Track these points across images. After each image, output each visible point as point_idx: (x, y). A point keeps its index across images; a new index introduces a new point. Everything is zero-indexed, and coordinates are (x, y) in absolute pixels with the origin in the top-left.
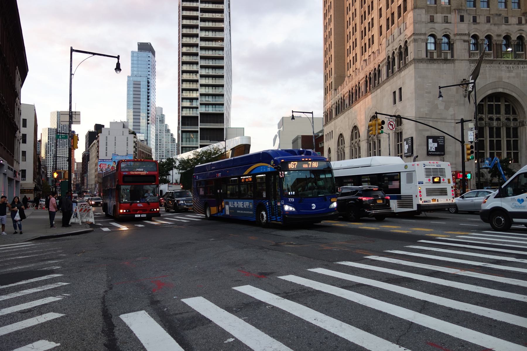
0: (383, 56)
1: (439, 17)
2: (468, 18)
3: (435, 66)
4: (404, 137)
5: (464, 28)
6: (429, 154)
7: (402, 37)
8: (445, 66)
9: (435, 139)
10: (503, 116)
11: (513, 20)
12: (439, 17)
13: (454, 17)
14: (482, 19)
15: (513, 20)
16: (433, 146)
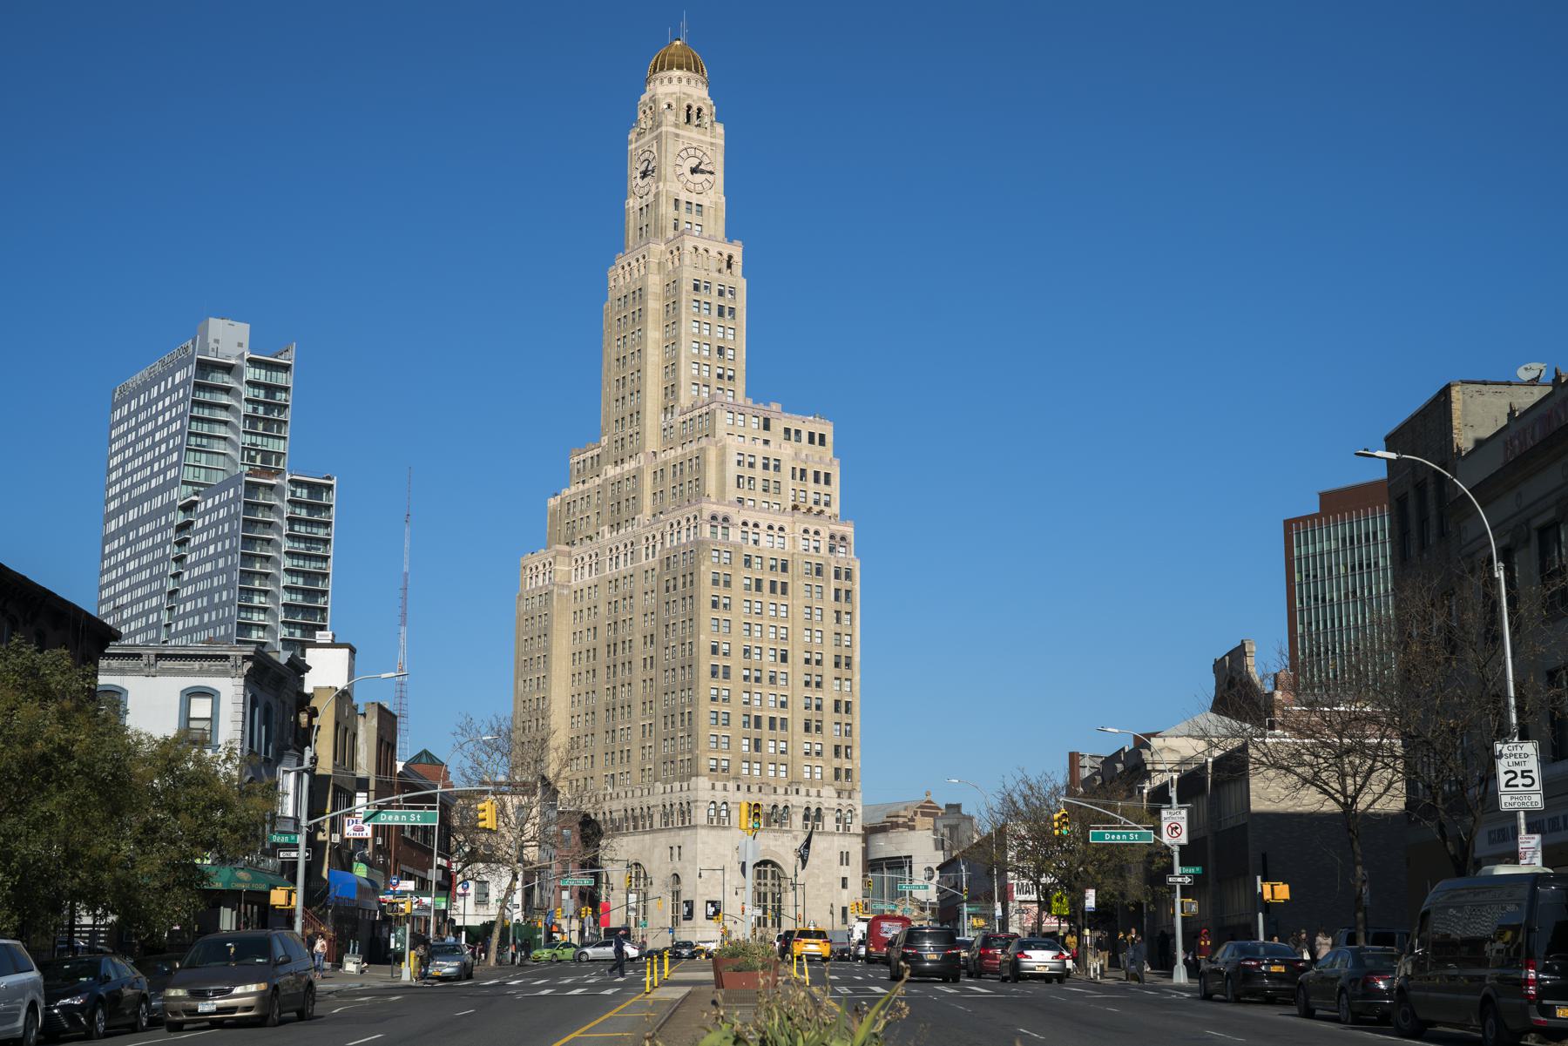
0: (656, 800)
1: (719, 785)
2: (744, 788)
3: (714, 832)
4: (683, 898)
5: (742, 797)
6: (708, 917)
7: (684, 795)
8: (723, 833)
9: (713, 903)
10: (769, 881)
11: (781, 791)
12: (719, 785)
13: (731, 785)
14: (755, 789)
15: (781, 791)
16: (711, 910)
